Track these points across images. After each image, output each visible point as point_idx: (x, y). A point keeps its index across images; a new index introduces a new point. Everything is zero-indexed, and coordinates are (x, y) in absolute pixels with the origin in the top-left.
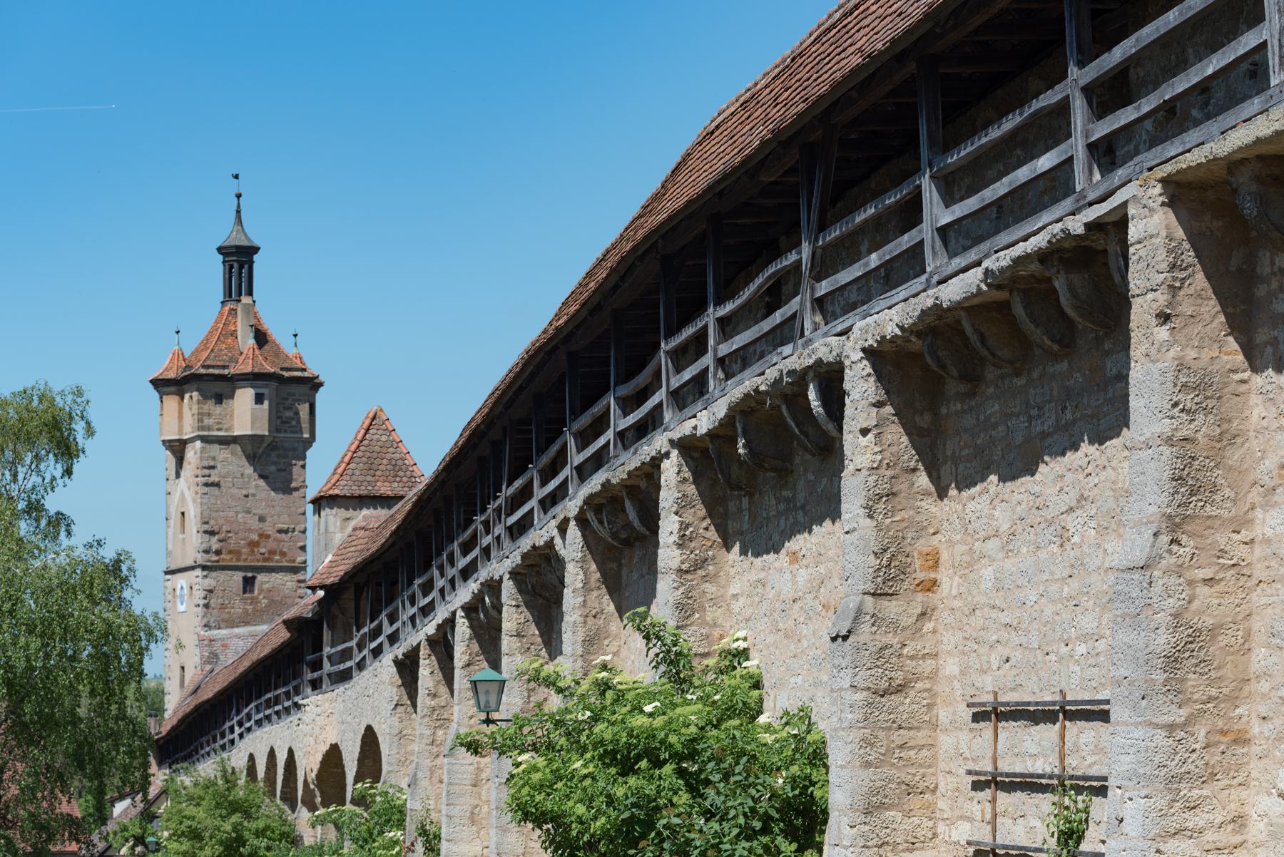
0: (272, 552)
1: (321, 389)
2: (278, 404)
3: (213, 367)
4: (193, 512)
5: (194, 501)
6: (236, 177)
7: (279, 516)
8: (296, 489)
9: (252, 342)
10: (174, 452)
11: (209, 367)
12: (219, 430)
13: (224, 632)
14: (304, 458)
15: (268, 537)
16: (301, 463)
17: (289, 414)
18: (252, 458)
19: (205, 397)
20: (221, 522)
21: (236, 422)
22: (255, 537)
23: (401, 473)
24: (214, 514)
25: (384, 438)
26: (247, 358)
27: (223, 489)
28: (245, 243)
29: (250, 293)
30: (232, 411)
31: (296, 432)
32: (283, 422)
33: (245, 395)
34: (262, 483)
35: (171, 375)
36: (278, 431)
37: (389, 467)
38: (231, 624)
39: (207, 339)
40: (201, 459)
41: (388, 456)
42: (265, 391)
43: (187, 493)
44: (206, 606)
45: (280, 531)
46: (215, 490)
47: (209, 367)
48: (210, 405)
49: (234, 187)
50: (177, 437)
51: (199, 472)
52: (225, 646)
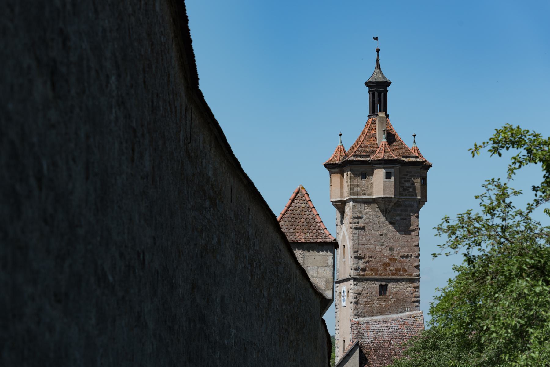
0: (398, 270)
1: (430, 169)
3: (360, 156)
5: (350, 239)
6: (376, 39)
7: (402, 247)
8: (413, 231)
9: (384, 140)
10: (338, 209)
11: (357, 156)
12: (364, 194)
13: (367, 319)
14: (418, 212)
15: (395, 260)
16: (416, 214)
18: (385, 212)
19: (355, 175)
20: (366, 251)
22: (387, 260)
23: (312, 228)
24: (361, 247)
25: (303, 205)
26: (381, 148)
27: (367, 231)
28: (382, 79)
29: (386, 111)
31: (413, 196)
32: (404, 189)
33: (380, 174)
34: (391, 227)
35: (336, 161)
36: (401, 194)
37: (305, 224)
38: (372, 314)
39: (359, 139)
40: (353, 212)
41: (305, 217)
42: (392, 171)
43: (346, 234)
44: (356, 303)
45: (403, 257)
46: (362, 232)
47: (357, 156)
48: (358, 180)
49: (375, 45)
50: (340, 199)
51: (352, 221)
52: (368, 328)
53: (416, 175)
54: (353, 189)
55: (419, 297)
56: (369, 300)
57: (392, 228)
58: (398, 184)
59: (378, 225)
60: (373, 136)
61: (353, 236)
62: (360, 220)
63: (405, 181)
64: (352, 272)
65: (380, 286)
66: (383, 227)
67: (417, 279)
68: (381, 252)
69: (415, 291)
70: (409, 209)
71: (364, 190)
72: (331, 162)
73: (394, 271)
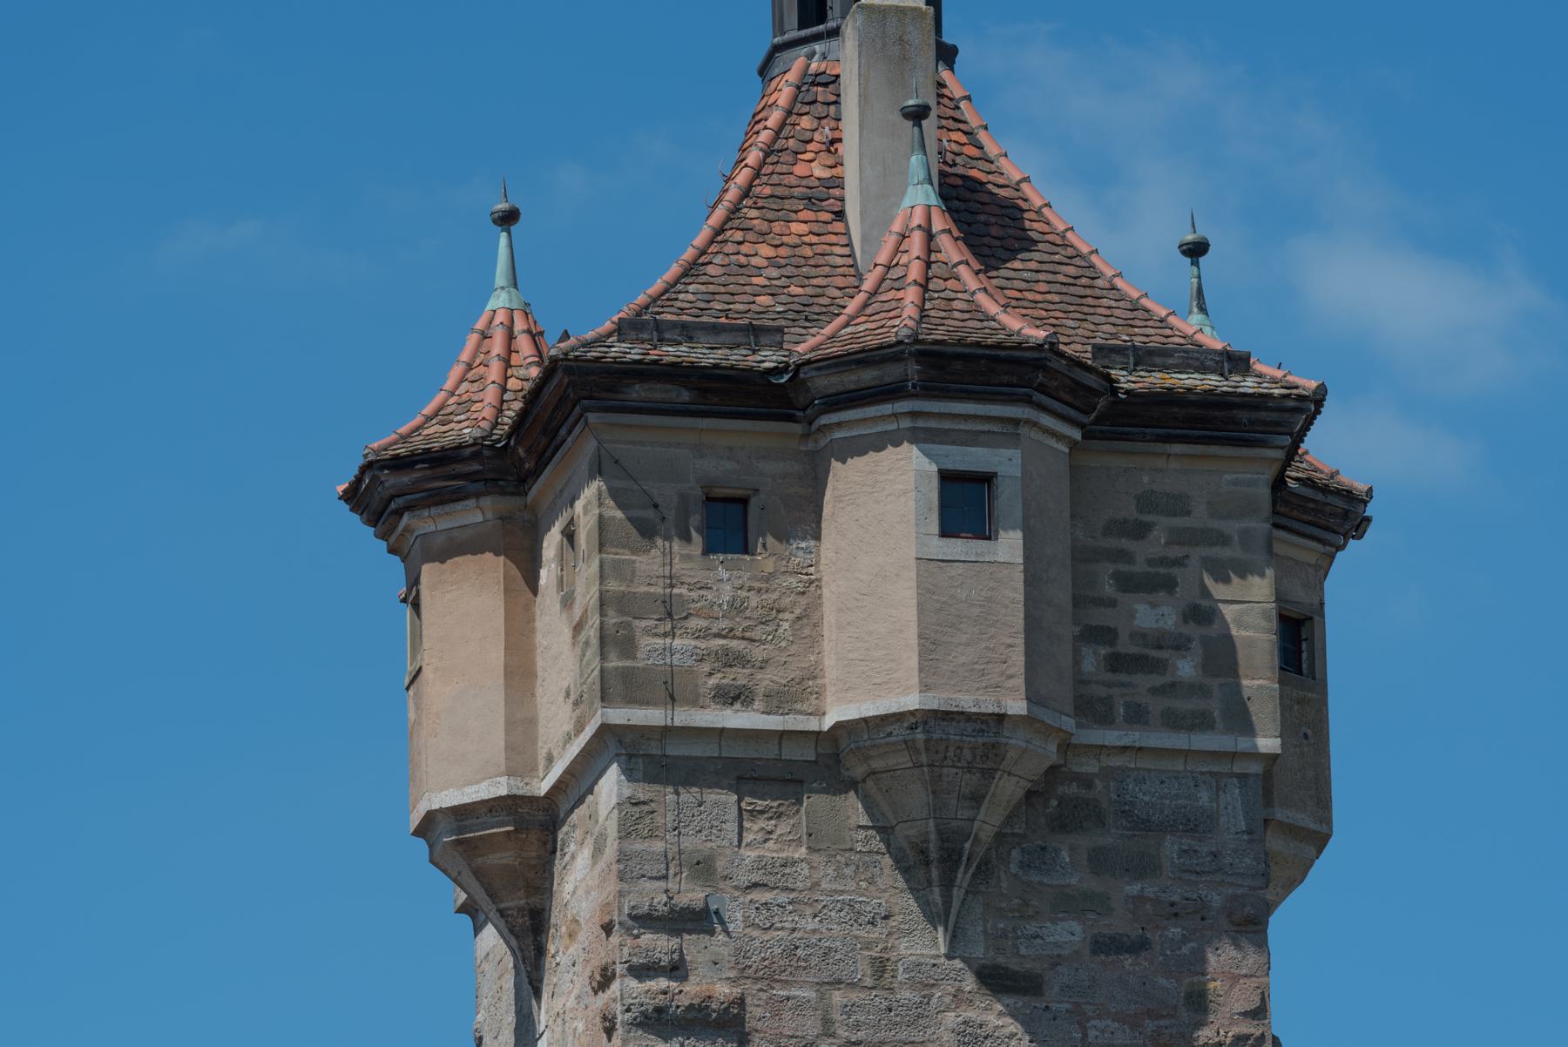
2: (1082, 556)
3: (687, 332)
9: (919, 197)
12: (733, 697)
17: (1152, 615)
18: (940, 867)
21: (835, 652)
30: (812, 585)
31: (1202, 722)
32: (1117, 663)
34: (994, 1016)
36: (1091, 709)
40: (627, 869)
42: (1004, 461)
50: (499, 787)
51: (619, 949)
53: (1231, 527)
54: (628, 646)
57: (1012, 1026)
58: (1062, 594)
59: (880, 999)
60: (811, 201)
62: (694, 947)
63: (1128, 584)
70: (1170, 847)
71: (730, 660)
72: (418, 443)
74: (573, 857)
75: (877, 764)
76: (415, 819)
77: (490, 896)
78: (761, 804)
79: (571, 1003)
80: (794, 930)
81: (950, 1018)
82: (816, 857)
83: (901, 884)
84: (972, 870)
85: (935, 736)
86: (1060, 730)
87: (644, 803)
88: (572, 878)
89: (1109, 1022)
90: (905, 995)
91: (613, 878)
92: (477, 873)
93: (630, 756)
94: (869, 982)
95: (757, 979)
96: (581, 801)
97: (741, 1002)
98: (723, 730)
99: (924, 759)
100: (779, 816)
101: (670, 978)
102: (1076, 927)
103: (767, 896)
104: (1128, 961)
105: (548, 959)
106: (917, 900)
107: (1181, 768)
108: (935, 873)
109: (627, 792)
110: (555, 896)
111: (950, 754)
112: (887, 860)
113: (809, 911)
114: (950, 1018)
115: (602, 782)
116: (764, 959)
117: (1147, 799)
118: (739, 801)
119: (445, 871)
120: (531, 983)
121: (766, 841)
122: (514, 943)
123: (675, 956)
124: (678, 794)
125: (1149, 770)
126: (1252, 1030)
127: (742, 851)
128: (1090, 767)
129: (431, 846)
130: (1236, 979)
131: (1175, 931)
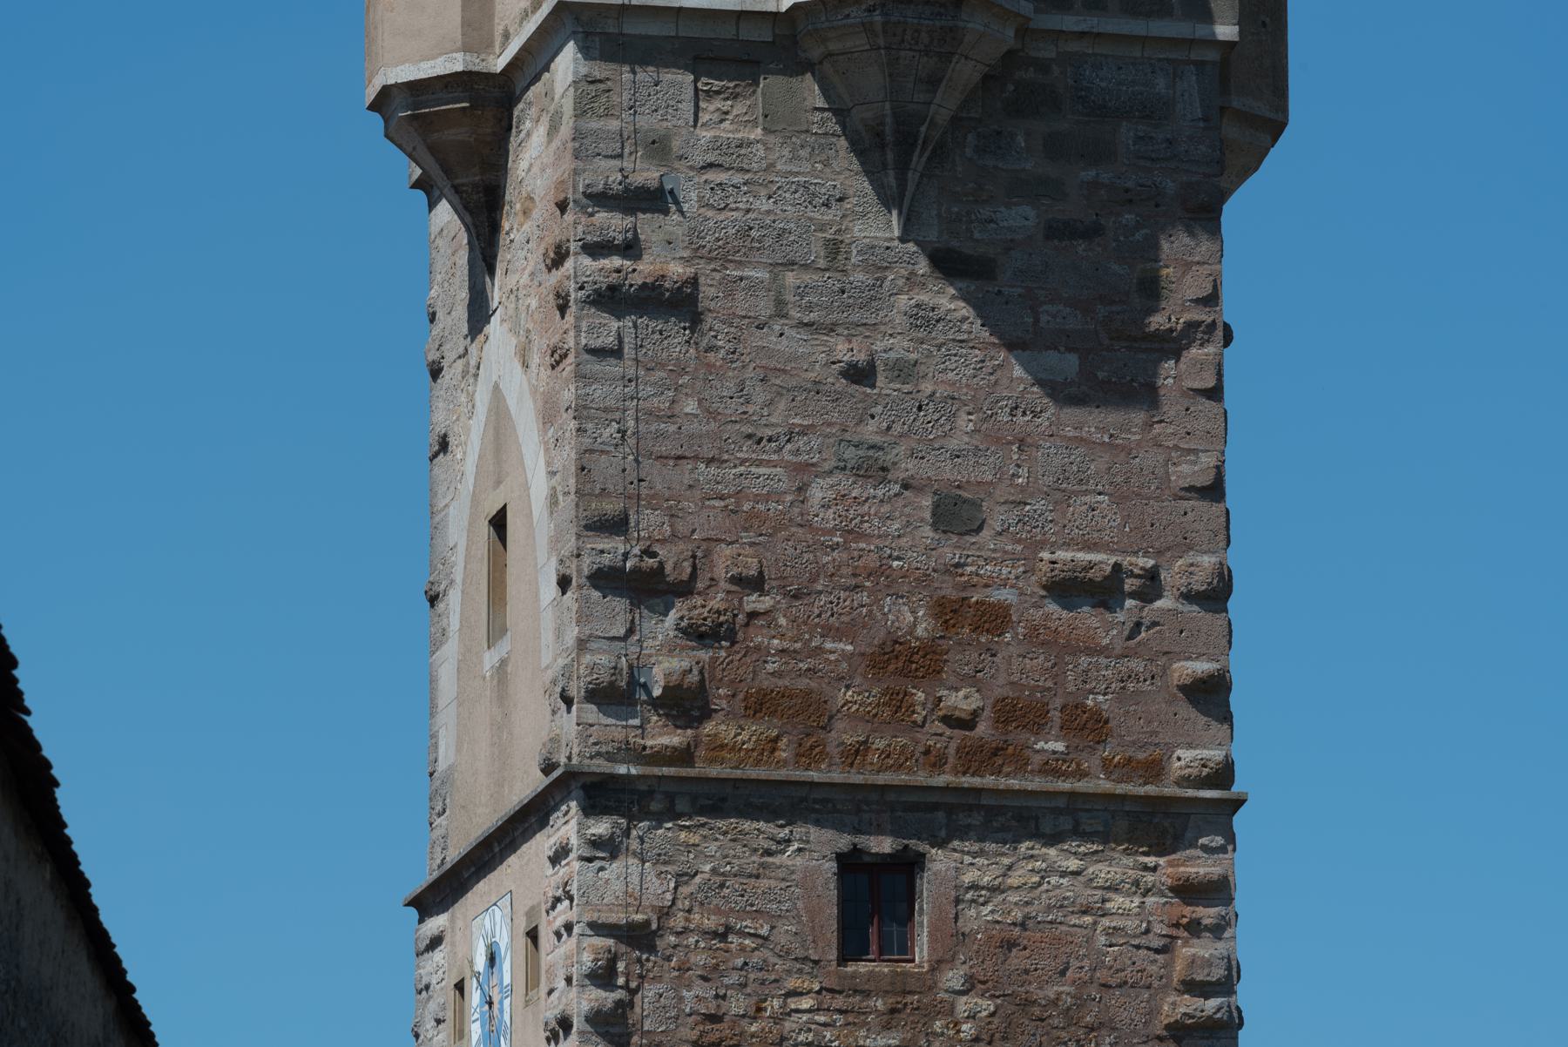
0: (1020, 714)
4: (538, 480)
5: (547, 417)
7: (1061, 496)
8: (1172, 344)
15: (995, 619)
20: (704, 521)
22: (913, 619)
24: (660, 477)
34: (946, 300)
40: (582, 148)
45: (1069, 589)
46: (672, 339)
50: (455, 63)
51: (573, 226)
55: (1226, 986)
56: (737, 1005)
57: (964, 310)
61: (580, 376)
62: (649, 226)
64: (568, 724)
65: (850, 864)
66: (873, 297)
67: (1210, 809)
68: (852, 534)
69: (1195, 928)
73: (983, 728)
74: (529, 134)
75: (833, 46)
76: (371, 94)
77: (445, 172)
78: (717, 84)
79: (525, 280)
80: (748, 211)
81: (903, 301)
82: (771, 139)
83: (856, 166)
84: (927, 154)
85: (893, 19)
86: (1018, 15)
87: (600, 81)
88: (527, 156)
89: (1061, 307)
90: (859, 277)
91: (568, 155)
92: (433, 150)
93: (587, 34)
94: (822, 263)
95: (711, 259)
96: (536, 78)
97: (694, 281)
98: (680, 9)
99: (882, 43)
100: (735, 96)
101: (625, 257)
102: (1030, 212)
103: (722, 177)
104: (1081, 247)
105: (502, 236)
106: (871, 182)
107: (1139, 55)
108: (890, 156)
109: (583, 70)
110: (510, 173)
111: (908, 37)
112: (843, 143)
113: (763, 192)
114: (903, 301)
115: (558, 59)
116: (718, 240)
117: (1103, 84)
118: (696, 81)
119: (400, 147)
120: (484, 260)
121: (722, 121)
122: (468, 219)
123: (629, 235)
124: (634, 73)
125: (1106, 56)
126: (1203, 317)
127: (698, 131)
128: (1047, 52)
129: (386, 121)
130: (1188, 266)
131: (1129, 218)
